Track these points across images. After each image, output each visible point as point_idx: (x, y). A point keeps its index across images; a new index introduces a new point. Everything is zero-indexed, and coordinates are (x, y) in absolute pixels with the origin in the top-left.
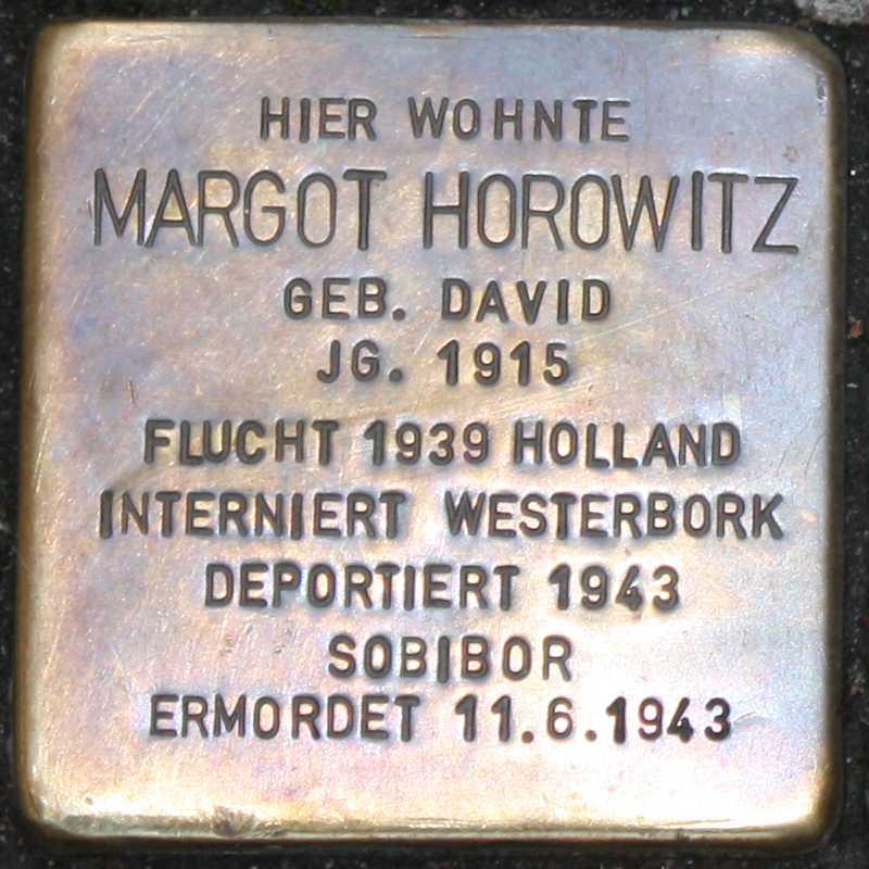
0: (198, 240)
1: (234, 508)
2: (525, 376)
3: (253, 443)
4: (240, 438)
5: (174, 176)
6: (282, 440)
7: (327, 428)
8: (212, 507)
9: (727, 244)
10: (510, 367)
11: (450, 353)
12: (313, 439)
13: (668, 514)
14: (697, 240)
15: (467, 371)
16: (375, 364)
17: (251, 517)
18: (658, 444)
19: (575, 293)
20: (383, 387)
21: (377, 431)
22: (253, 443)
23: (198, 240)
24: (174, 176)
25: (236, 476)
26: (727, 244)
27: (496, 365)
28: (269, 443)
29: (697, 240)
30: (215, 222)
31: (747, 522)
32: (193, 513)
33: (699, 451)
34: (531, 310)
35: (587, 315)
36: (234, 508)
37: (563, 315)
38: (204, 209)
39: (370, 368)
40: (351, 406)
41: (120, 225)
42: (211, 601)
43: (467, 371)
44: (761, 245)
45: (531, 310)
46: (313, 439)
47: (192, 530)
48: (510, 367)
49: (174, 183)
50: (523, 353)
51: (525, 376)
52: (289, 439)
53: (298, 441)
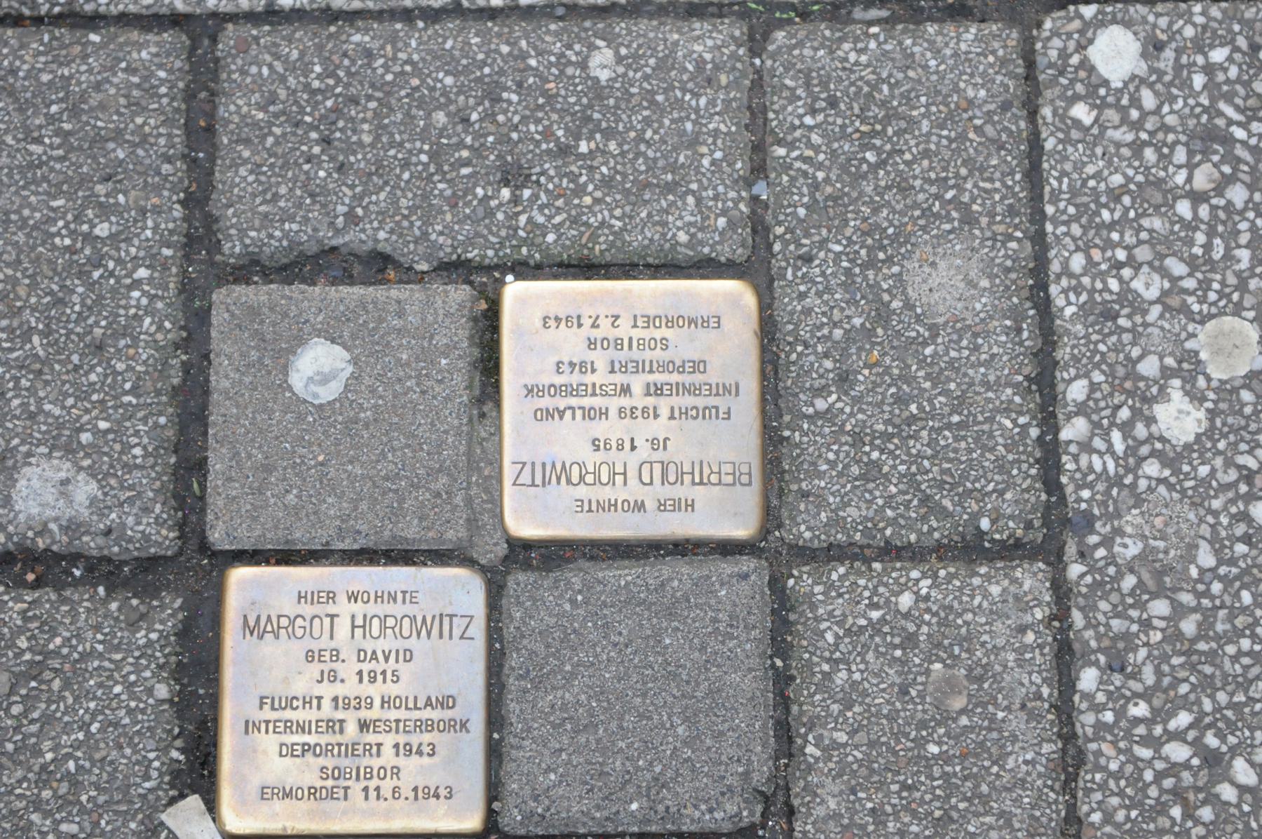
0: (277, 637)
1: (288, 726)
2: (384, 681)
3: (295, 703)
4: (290, 703)
5: (269, 617)
6: (305, 703)
7: (319, 698)
8: (281, 724)
9: (451, 637)
10: (380, 678)
11: (360, 673)
12: (315, 702)
13: (432, 725)
14: (441, 636)
15: (366, 678)
16: (335, 677)
17: (294, 729)
18: (429, 703)
19: (401, 653)
20: (338, 683)
21: (335, 699)
22: (295, 703)
23: (277, 637)
24: (269, 617)
25: (289, 714)
26: (451, 637)
27: (375, 677)
28: (300, 703)
29: (441, 636)
30: (283, 631)
31: (458, 727)
32: (275, 727)
33: (442, 705)
34: (387, 659)
35: (405, 661)
36: (288, 726)
37: (397, 661)
38: (279, 627)
39: (333, 677)
40: (327, 691)
41: (252, 633)
42: (281, 755)
43: (366, 678)
44: (462, 637)
45: (387, 659)
46: (315, 702)
47: (274, 732)
48: (380, 678)
49: (269, 618)
50: (384, 673)
51: (384, 681)
52: (307, 702)
53: (310, 703)
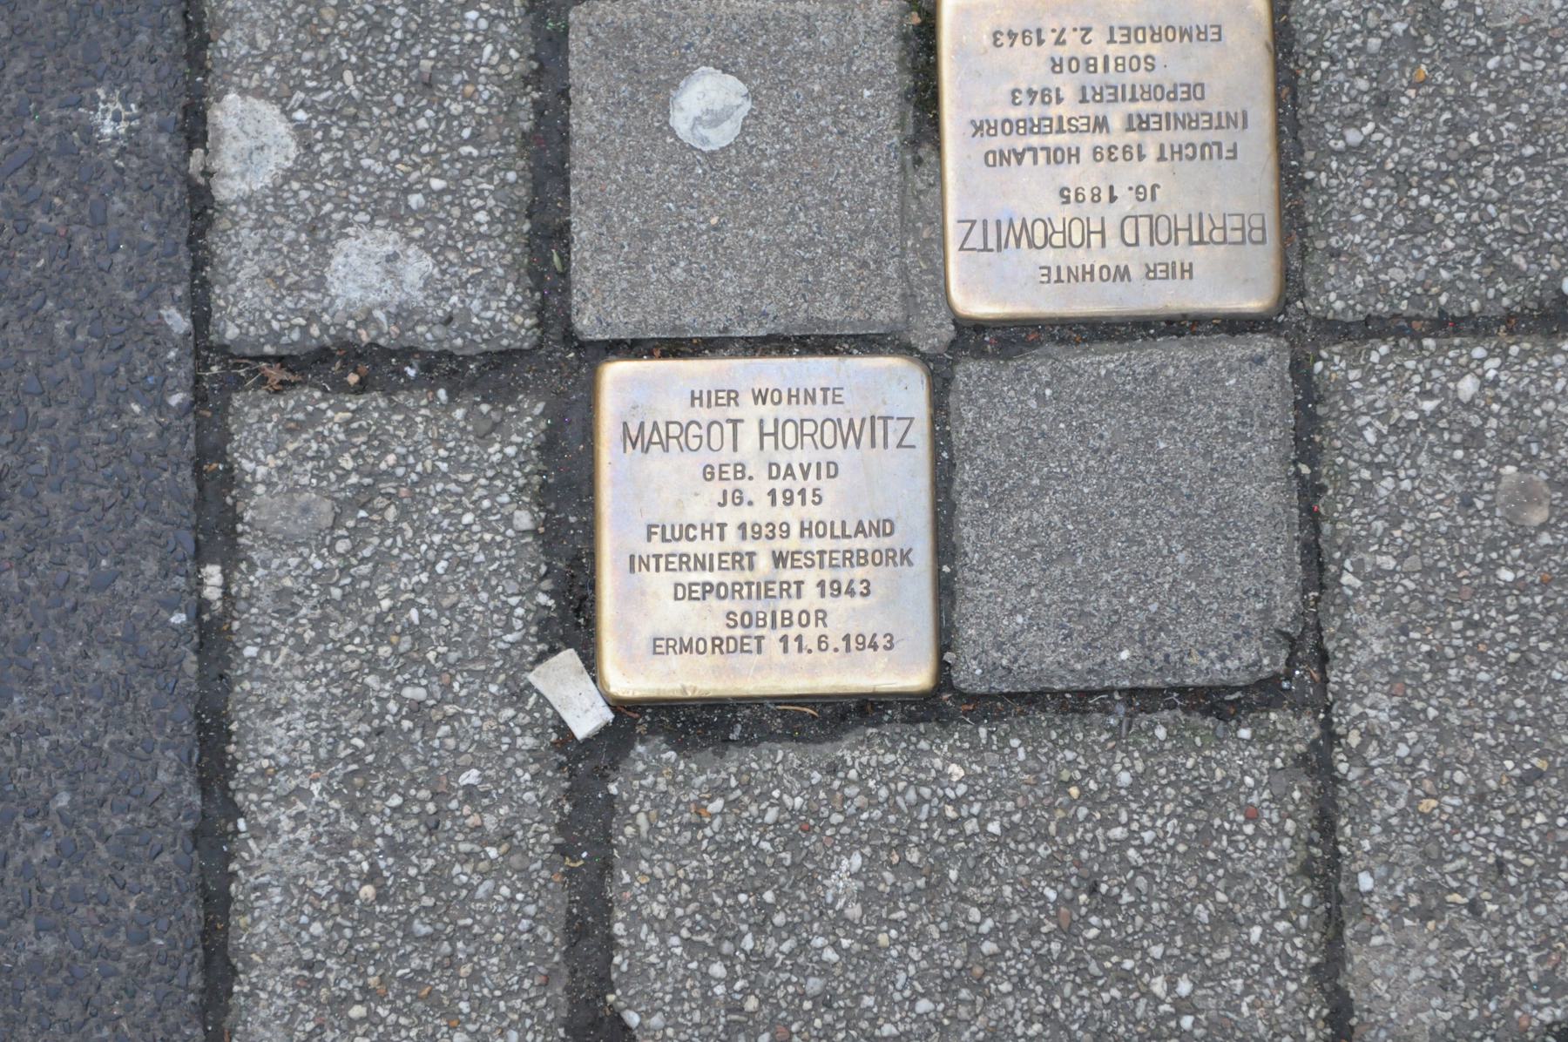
0: (666, 450)
5: (655, 424)
6: (704, 531)
7: (722, 526)
8: (675, 559)
9: (886, 445)
10: (798, 499)
11: (772, 493)
12: (716, 530)
14: (873, 444)
18: (860, 529)
20: (744, 506)
21: (742, 527)
22: (692, 533)
23: (666, 450)
24: (655, 424)
25: (684, 546)
26: (886, 445)
27: (792, 498)
28: (698, 532)
29: (873, 444)
30: (673, 442)
31: (898, 559)
34: (805, 475)
35: (829, 476)
37: (819, 477)
38: (668, 437)
39: (738, 499)
40: (732, 516)
41: (634, 445)
42: (676, 598)
44: (899, 446)
45: (805, 475)
46: (716, 530)
47: (667, 569)
48: (798, 499)
49: (655, 425)
50: (802, 492)
51: (803, 502)
52: (706, 531)
53: (711, 531)
